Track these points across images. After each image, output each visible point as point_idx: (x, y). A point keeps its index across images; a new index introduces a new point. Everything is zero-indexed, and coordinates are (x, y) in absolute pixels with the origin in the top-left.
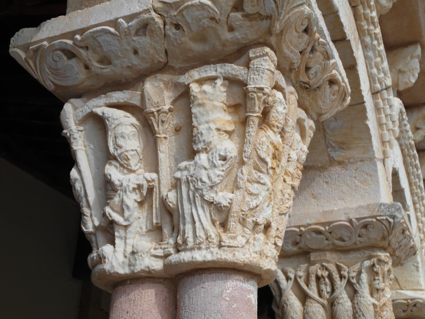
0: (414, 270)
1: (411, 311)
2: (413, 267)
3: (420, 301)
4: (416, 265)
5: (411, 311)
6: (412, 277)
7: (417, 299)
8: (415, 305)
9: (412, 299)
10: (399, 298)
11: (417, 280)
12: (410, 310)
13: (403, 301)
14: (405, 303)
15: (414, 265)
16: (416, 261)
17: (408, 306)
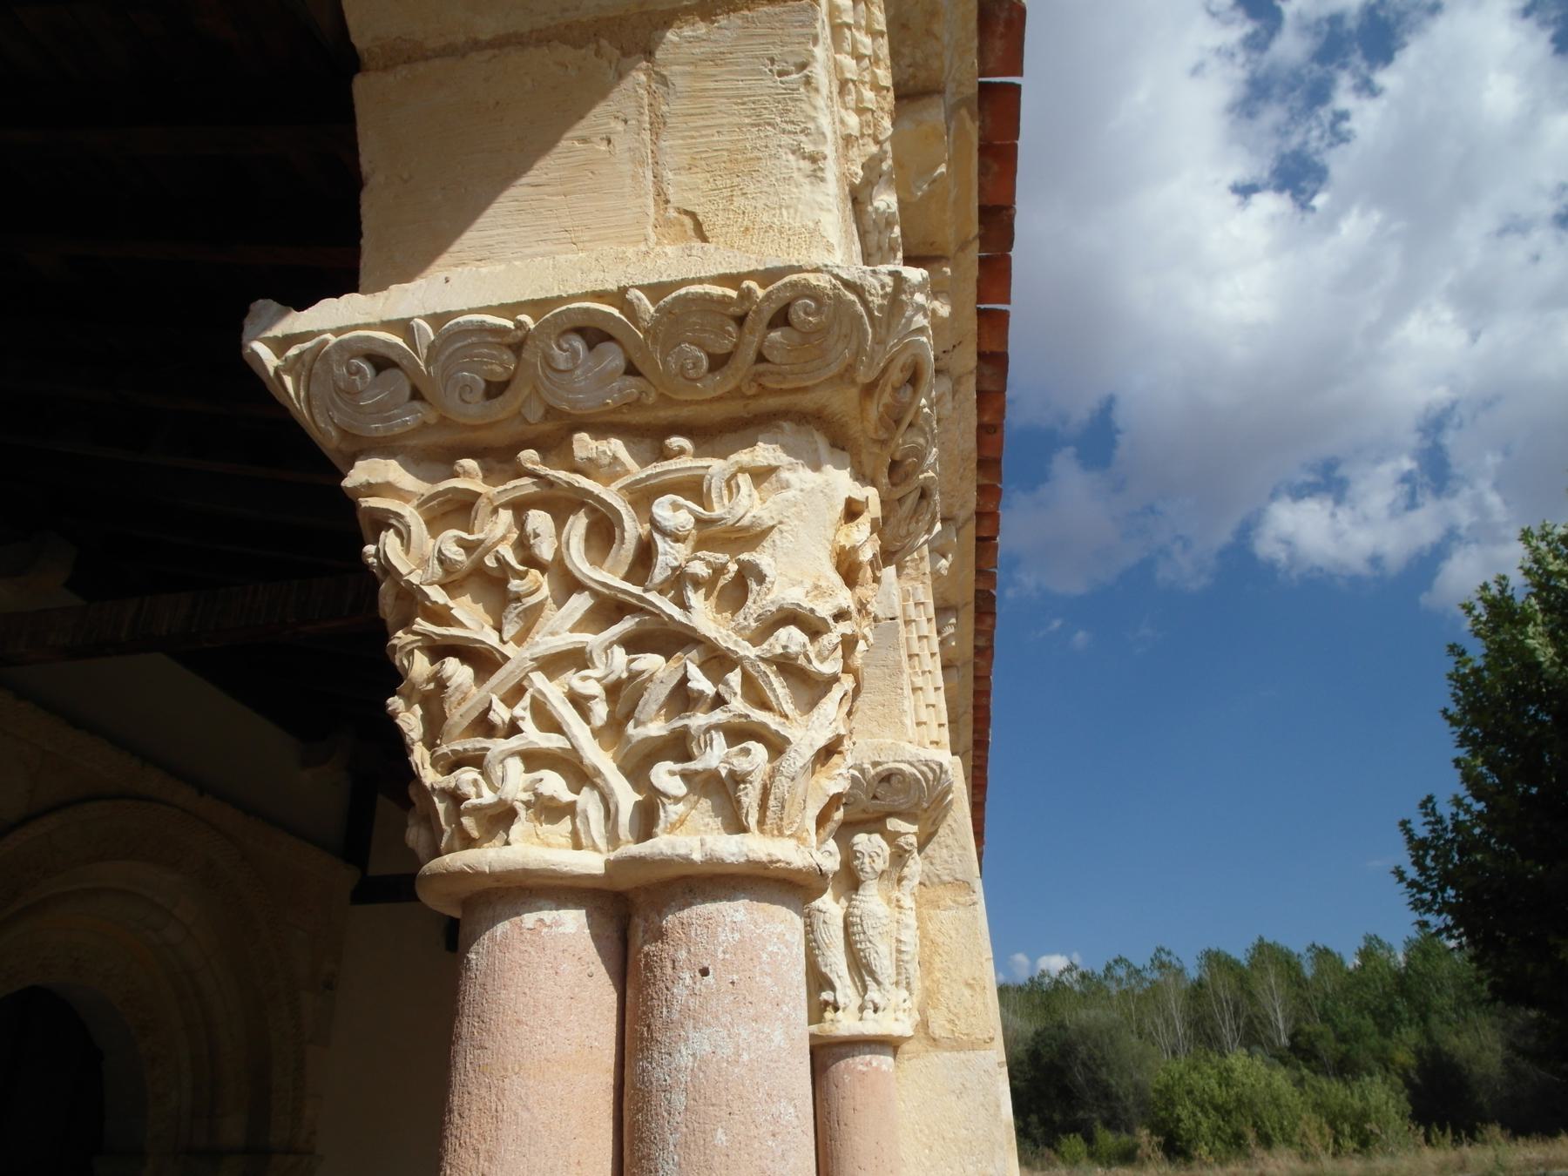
0: (796, 175)
1: (761, 358)
2: (791, 157)
3: (822, 281)
4: (809, 148)
5: (761, 358)
6: (784, 212)
7: (800, 269)
8: (781, 318)
9: (767, 276)
10: (691, 276)
11: (811, 225)
12: (751, 354)
13: (717, 290)
14: (724, 301)
15: (797, 151)
16: (811, 125)
17: (740, 320)
